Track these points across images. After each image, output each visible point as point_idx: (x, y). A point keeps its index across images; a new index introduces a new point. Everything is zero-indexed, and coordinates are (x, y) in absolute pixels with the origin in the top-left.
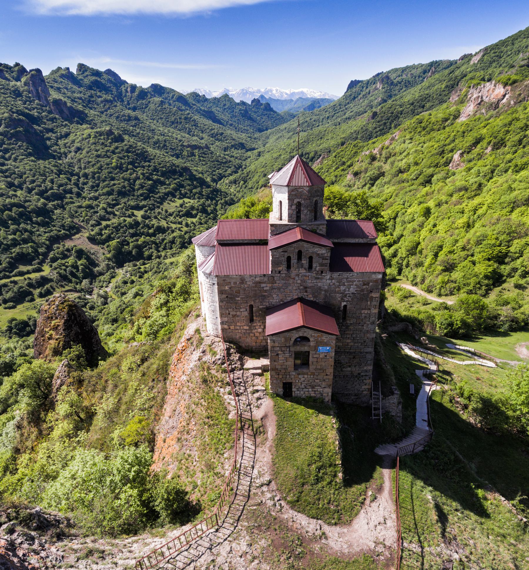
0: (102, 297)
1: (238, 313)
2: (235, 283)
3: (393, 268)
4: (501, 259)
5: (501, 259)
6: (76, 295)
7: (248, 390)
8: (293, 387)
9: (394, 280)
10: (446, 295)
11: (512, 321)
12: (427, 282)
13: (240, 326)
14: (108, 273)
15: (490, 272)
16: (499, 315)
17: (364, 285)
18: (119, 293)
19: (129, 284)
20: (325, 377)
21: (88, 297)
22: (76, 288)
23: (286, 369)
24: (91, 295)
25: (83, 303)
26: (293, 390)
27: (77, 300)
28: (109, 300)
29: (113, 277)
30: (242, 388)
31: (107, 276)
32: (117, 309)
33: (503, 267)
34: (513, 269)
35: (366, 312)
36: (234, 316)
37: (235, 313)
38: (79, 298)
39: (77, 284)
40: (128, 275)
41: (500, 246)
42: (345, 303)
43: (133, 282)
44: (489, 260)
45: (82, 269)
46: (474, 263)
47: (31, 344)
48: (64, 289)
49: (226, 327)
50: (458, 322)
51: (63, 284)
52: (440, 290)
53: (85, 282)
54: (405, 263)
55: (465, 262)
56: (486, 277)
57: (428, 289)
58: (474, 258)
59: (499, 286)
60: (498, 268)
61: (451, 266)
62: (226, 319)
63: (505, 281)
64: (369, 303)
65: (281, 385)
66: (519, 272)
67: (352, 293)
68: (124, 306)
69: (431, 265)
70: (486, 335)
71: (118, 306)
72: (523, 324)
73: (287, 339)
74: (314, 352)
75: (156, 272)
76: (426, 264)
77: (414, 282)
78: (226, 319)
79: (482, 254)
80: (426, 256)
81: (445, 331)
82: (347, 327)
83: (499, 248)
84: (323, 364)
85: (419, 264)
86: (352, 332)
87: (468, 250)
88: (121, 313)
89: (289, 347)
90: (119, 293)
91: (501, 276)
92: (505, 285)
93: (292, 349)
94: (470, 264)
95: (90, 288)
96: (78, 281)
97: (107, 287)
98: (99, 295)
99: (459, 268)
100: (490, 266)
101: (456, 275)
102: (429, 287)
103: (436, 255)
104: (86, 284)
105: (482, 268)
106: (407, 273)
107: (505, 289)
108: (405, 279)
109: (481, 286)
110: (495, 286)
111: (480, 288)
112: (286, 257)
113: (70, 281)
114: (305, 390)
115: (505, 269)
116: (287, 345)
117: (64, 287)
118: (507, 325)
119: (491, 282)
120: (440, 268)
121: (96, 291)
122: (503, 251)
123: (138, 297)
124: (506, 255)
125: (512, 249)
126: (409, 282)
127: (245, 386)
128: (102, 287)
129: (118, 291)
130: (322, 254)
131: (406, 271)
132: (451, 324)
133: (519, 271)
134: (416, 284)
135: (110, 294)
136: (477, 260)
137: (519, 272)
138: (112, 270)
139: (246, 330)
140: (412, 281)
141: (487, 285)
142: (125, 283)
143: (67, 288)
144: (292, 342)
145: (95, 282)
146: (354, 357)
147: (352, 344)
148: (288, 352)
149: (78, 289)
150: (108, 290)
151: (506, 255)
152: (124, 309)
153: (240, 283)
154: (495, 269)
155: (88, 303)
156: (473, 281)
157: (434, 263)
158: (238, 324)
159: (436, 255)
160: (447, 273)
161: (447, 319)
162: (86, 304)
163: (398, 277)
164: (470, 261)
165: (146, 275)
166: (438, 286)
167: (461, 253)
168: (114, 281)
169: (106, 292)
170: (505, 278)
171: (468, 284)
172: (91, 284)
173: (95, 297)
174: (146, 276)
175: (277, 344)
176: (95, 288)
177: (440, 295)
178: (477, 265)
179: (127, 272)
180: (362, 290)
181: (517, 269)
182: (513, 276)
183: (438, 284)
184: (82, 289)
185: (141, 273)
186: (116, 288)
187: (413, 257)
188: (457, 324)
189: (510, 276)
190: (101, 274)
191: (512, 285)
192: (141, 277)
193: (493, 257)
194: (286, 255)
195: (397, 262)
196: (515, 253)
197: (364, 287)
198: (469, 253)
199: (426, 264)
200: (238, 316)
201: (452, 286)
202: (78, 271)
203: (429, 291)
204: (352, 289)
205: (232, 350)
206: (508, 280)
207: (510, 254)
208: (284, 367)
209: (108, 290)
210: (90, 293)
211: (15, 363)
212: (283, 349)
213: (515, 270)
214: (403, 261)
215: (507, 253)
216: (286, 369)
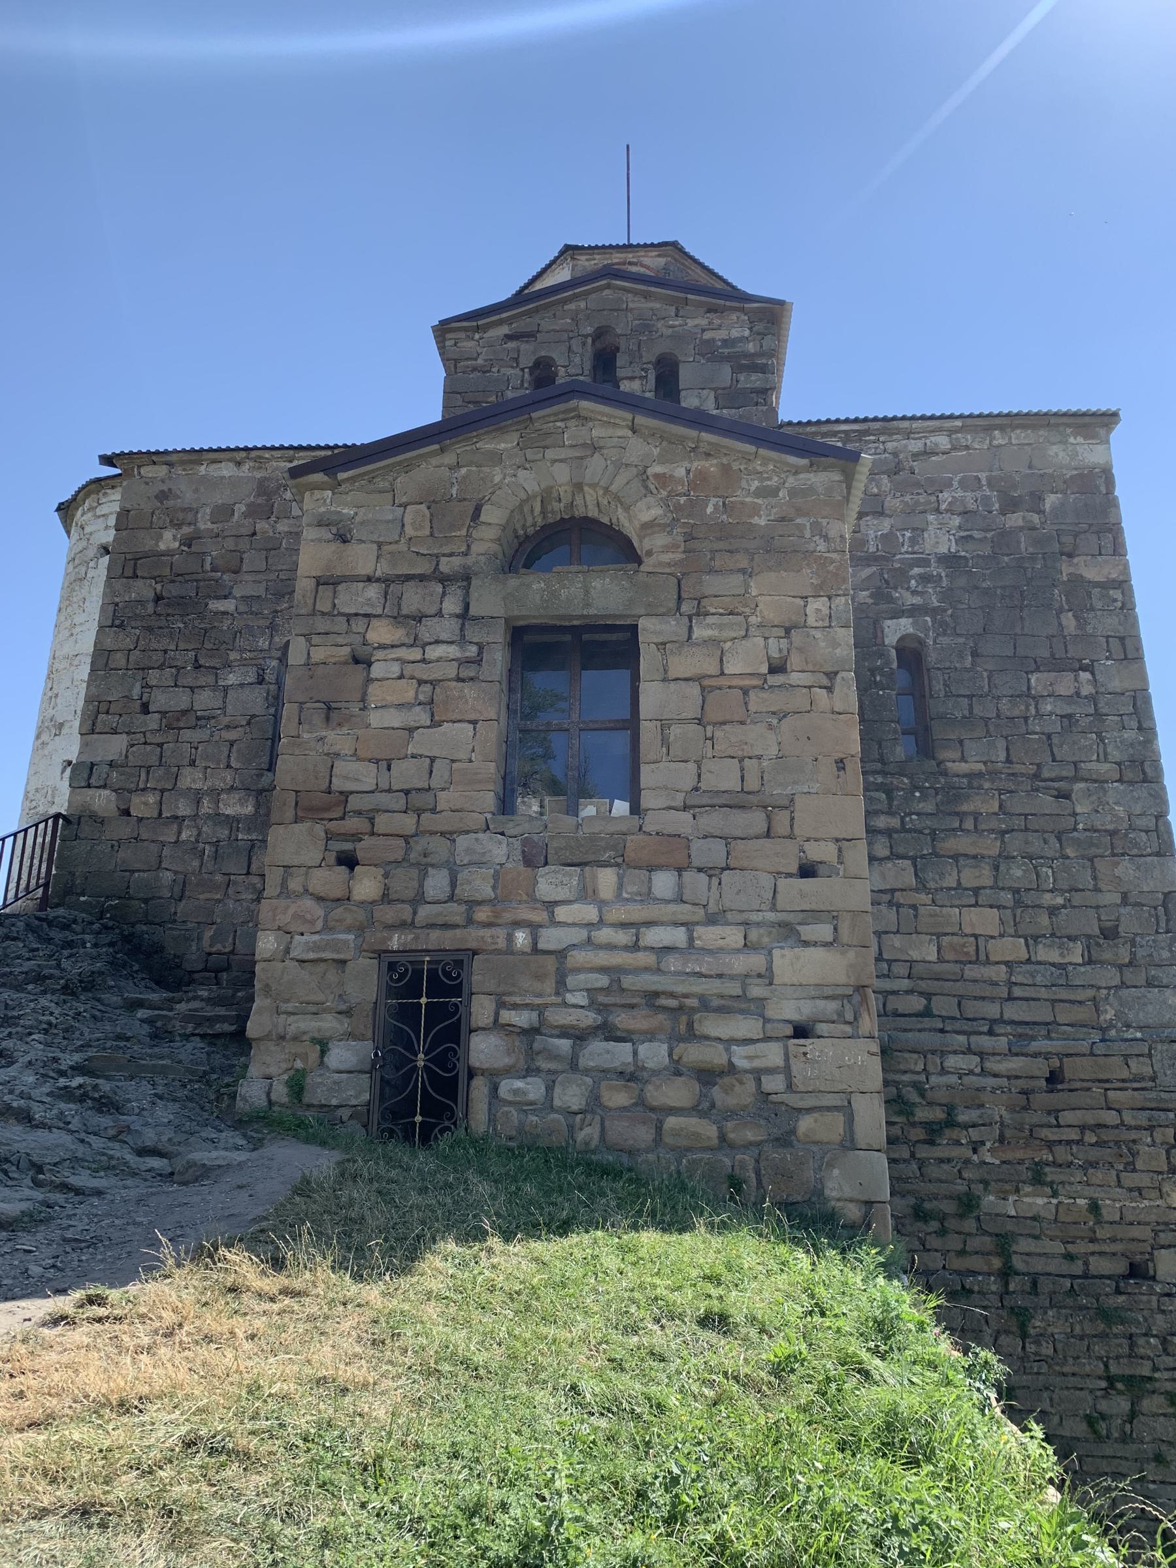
1: (205, 700)
2: (223, 512)
8: (481, 1010)
13: (197, 798)
17: (1010, 505)
20: (796, 892)
23: (417, 801)
26: (483, 1049)
35: (1065, 685)
36: (173, 721)
37: (180, 700)
42: (904, 626)
49: (102, 801)
62: (114, 747)
64: (1069, 620)
65: (365, 985)
67: (949, 560)
73: (454, 511)
74: (671, 627)
78: (114, 747)
82: (952, 795)
84: (763, 741)
86: (990, 846)
89: (465, 578)
93: (488, 600)
112: (527, 361)
114: (599, 1053)
116: (445, 566)
130: (726, 342)
139: (232, 822)
144: (486, 540)
146: (1054, 1078)
147: (1015, 948)
148: (447, 628)
153: (253, 512)
158: (191, 779)
175: (362, 558)
180: (1005, 537)
194: (528, 353)
197: (1015, 520)
200: (201, 721)
204: (940, 539)
208: (406, 774)
212: (413, 599)
216: (417, 801)
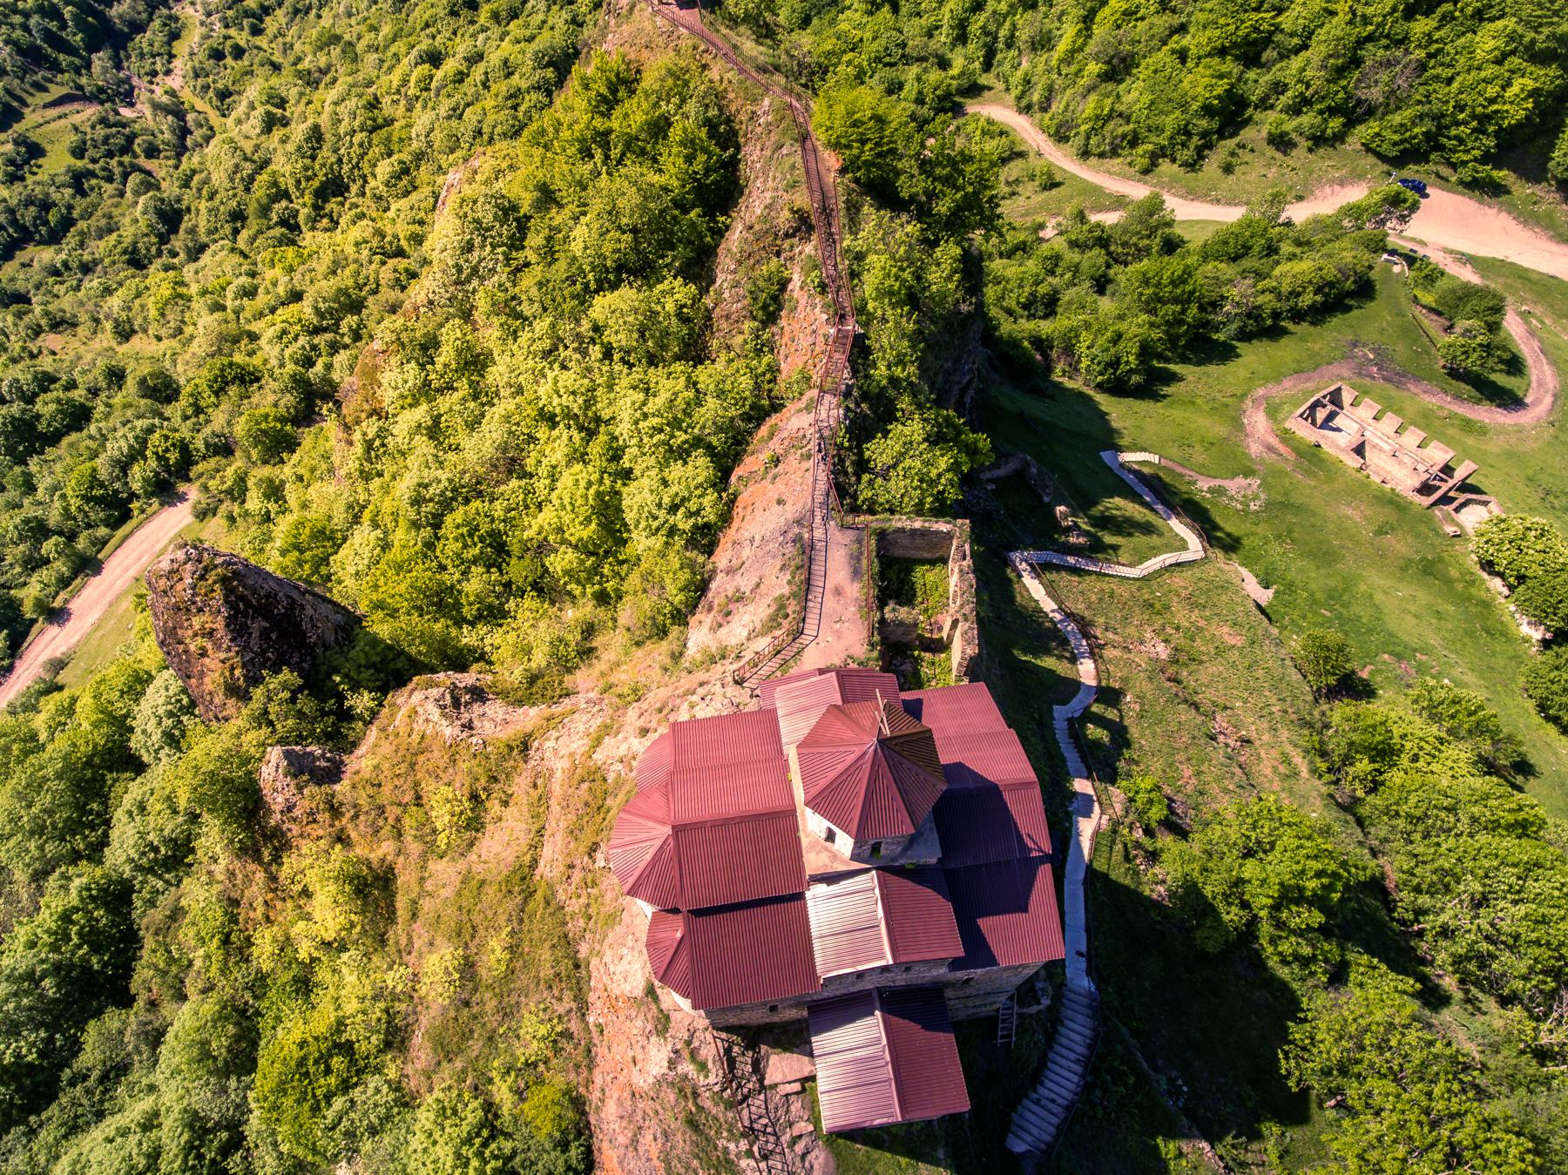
0: (167, 110)
3: (971, 47)
4: (1251, 52)
5: (1251, 52)
6: (91, 112)
7: (783, 1139)
9: (974, 90)
10: (1101, 155)
11: (1249, 316)
12: (1057, 107)
14: (156, 24)
15: (1218, 97)
16: (1223, 298)
18: (211, 93)
19: (229, 61)
21: (127, 113)
22: (80, 88)
24: (132, 105)
25: (120, 141)
27: (101, 132)
28: (190, 117)
29: (175, 36)
30: (772, 1139)
31: (153, 35)
32: (232, 180)
33: (1251, 75)
34: (1277, 84)
38: (103, 121)
39: (78, 72)
40: (218, 26)
41: (1257, 10)
43: (239, 53)
44: (1222, 52)
45: (75, 17)
46: (1183, 55)
47: (43, 322)
48: (48, 97)
50: (1131, 358)
51: (38, 77)
52: (1088, 138)
53: (100, 60)
54: (1003, 33)
55: (1160, 55)
56: (1208, 110)
57: (1058, 131)
58: (1186, 41)
59: (1232, 136)
60: (1239, 79)
61: (1123, 60)
63: (1249, 121)
66: (1285, 99)
68: (248, 168)
69: (1072, 52)
70: (1184, 360)
71: (231, 169)
72: (1269, 322)
75: (296, 11)
76: (1062, 47)
77: (1024, 103)
79: (1208, 33)
80: (1063, 13)
81: (1100, 379)
83: (1255, 16)
85: (1043, 42)
87: (1174, 11)
88: (247, 190)
90: (211, 93)
91: (1242, 103)
92: (1247, 134)
94: (1171, 61)
95: (120, 82)
96: (77, 61)
97: (168, 72)
98: (156, 107)
99: (1143, 72)
100: (1221, 76)
101: (1134, 94)
102: (1059, 126)
103: (1088, 20)
104: (105, 70)
105: (1201, 84)
106: (1007, 67)
107: (1244, 147)
108: (1001, 86)
109: (1189, 134)
110: (1222, 137)
111: (1183, 145)
113: (56, 67)
115: (1257, 82)
117: (46, 90)
118: (1235, 326)
119: (1215, 125)
120: (1094, 68)
121: (142, 95)
122: (1265, 27)
123: (278, 133)
124: (1267, 40)
125: (1286, 21)
126: (1010, 98)
127: (775, 1134)
128: (154, 74)
129: (206, 87)
131: (1005, 58)
132: (1115, 363)
133: (1290, 93)
134: (1028, 109)
135: (187, 96)
136: (1193, 51)
137: (1285, 99)
138: (165, 11)
140: (1019, 98)
141: (1204, 135)
142: (217, 55)
143: (56, 91)
145: (128, 57)
149: (88, 90)
150: (174, 82)
151: (1267, 40)
152: (252, 179)
154: (1232, 86)
155: (134, 136)
156: (1171, 121)
157: (1081, 49)
159: (1088, 20)
160: (1110, 86)
161: (1107, 350)
162: (130, 139)
163: (984, 80)
164: (1173, 52)
165: (268, 19)
166: (1084, 128)
167: (1156, 20)
168: (181, 48)
169: (172, 93)
170: (1250, 111)
171: (1160, 130)
172: (119, 67)
173: (148, 112)
174: (270, 24)
176: (135, 81)
177: (1085, 154)
178: (1190, 64)
179: (209, 14)
181: (1286, 85)
182: (1272, 107)
183: (1086, 121)
184: (101, 90)
185: (254, 15)
186: (197, 76)
187: (1029, 15)
188: (1127, 363)
189: (1264, 104)
190: (139, 28)
191: (1264, 133)
192: (257, 31)
193: (1235, 45)
195: (983, 27)
196: (1291, 35)
198: (1176, 20)
199: (1062, 47)
201: (1120, 131)
202: (64, 26)
203: (1060, 137)
205: (736, 1049)
206: (1258, 116)
207: (1278, 37)
209: (174, 82)
210: (128, 98)
211: (38, 417)
213: (1279, 88)
214: (1000, 25)
215: (1271, 33)
